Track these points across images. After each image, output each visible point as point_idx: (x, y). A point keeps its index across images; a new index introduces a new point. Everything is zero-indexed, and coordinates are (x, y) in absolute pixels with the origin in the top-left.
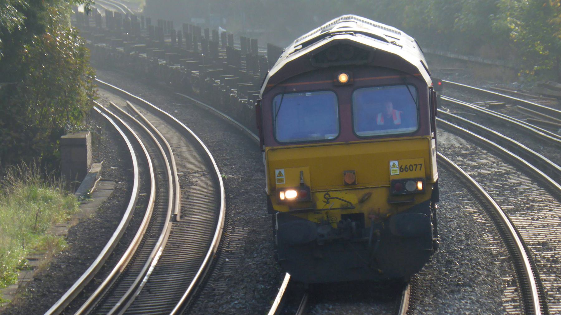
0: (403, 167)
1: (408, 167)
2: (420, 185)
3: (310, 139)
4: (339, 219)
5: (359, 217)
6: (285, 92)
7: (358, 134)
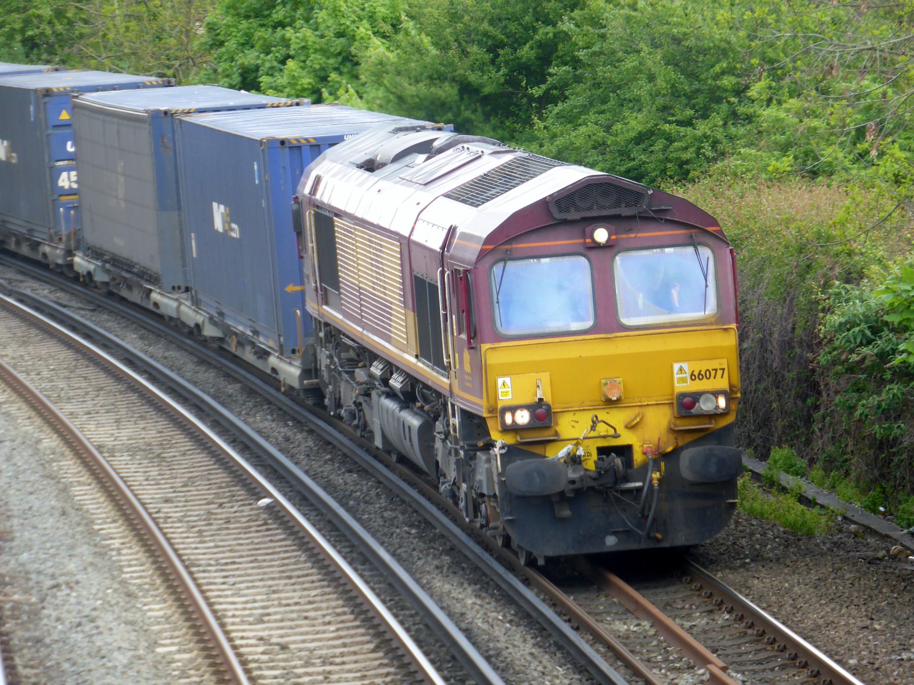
0: (696, 373)
1: (703, 373)
2: (722, 402)
3: (547, 330)
4: (595, 456)
5: (625, 451)
6: (507, 257)
7: (626, 321)
